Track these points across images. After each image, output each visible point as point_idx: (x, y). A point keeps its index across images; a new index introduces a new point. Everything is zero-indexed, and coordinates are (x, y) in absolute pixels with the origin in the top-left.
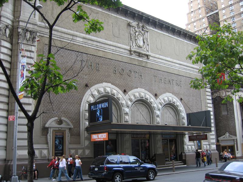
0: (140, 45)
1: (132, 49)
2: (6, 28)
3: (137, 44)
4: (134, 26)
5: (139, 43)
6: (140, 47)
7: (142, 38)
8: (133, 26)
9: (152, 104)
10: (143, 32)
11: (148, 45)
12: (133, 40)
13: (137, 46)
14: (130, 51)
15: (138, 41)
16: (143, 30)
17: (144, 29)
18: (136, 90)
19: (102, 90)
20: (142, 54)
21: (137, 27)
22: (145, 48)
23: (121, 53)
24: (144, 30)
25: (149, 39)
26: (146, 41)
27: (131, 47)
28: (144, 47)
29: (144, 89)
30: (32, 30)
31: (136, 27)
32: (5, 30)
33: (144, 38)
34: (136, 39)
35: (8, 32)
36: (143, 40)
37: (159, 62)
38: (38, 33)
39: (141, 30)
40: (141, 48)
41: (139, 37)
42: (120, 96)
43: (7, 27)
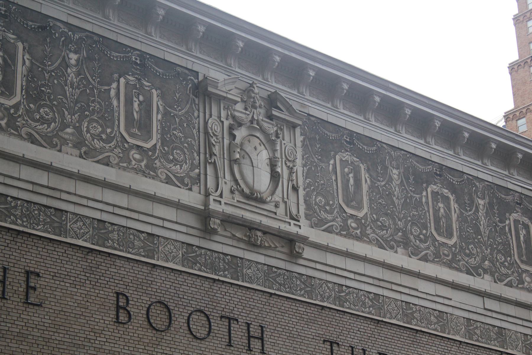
0: (256, 187)
1: (213, 206)
3: (240, 181)
4: (225, 98)
5: (250, 180)
6: (253, 197)
8: (220, 99)
10: (271, 128)
11: (295, 189)
12: (223, 164)
13: (242, 192)
14: (204, 216)
15: (247, 171)
16: (270, 117)
17: (275, 113)
20: (265, 233)
21: (242, 101)
22: (282, 206)
23: (160, 223)
24: (278, 118)
25: (299, 162)
26: (286, 174)
27: (211, 198)
28: (277, 197)
31: (236, 102)
33: (278, 155)
34: (236, 161)
36: (273, 165)
37: (352, 276)
39: (260, 114)
40: (262, 201)
41: (248, 148)
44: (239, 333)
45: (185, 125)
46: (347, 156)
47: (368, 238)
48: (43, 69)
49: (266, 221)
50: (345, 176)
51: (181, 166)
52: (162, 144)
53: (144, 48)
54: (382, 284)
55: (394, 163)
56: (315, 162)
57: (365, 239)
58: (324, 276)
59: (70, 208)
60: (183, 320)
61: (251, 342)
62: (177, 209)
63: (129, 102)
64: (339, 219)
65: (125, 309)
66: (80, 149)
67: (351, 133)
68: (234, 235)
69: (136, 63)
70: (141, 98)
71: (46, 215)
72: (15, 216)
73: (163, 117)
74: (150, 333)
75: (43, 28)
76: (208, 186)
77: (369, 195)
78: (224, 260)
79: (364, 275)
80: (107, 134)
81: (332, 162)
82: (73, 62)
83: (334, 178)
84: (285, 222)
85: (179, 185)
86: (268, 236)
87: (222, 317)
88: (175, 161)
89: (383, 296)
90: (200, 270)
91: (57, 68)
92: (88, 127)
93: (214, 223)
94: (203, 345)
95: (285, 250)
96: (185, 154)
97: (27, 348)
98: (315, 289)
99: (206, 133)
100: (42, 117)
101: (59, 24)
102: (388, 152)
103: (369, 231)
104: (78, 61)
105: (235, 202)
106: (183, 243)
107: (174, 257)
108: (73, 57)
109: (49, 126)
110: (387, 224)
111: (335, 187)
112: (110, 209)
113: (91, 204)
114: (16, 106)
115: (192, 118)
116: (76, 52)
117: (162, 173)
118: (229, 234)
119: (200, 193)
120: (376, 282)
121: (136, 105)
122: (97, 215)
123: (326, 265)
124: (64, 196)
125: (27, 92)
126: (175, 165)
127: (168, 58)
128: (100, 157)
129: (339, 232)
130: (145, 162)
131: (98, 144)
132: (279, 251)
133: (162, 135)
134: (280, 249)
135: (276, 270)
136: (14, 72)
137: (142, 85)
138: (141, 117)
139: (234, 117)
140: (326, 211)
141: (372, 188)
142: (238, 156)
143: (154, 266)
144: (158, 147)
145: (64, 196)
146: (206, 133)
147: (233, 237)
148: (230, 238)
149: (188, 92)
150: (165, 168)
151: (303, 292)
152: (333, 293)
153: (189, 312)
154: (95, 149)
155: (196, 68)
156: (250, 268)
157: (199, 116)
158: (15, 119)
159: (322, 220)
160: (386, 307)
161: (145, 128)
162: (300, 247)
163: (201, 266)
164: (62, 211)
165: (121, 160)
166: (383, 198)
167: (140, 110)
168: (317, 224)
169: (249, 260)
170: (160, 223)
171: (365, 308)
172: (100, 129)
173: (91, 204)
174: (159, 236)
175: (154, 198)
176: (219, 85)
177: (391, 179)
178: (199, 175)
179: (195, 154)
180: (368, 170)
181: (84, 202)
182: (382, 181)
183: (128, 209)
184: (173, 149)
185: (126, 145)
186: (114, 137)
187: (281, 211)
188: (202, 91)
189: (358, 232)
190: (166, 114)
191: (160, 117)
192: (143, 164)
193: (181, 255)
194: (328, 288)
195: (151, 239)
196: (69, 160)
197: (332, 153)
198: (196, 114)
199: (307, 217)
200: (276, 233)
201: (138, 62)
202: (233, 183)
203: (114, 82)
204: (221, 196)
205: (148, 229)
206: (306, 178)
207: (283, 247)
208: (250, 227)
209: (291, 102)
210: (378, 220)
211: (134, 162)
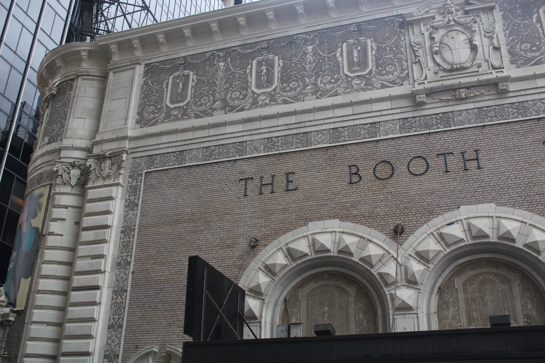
0: (455, 62)
2: (71, 168)
8: (418, 22)
9: (539, 253)
10: (468, 19)
11: (497, 49)
13: (444, 70)
15: (447, 55)
16: (467, 13)
17: (468, 8)
18: (450, 216)
19: (302, 246)
20: (468, 88)
23: (379, 113)
29: (493, 205)
30: (114, 153)
32: (69, 173)
34: (436, 53)
35: (75, 173)
36: (471, 41)
38: (124, 155)
40: (466, 68)
41: (446, 41)
42: (373, 251)
43: (73, 165)
44: (454, 162)
45: (394, 49)
48: (291, 63)
49: (463, 81)
51: (393, 75)
52: (377, 68)
53: (359, 20)
56: (517, 23)
58: (537, 97)
59: (313, 129)
60: (404, 168)
61: (467, 164)
63: (350, 54)
65: (356, 173)
66: (316, 95)
69: (355, 31)
70: (359, 48)
71: (297, 139)
72: (277, 146)
74: (378, 182)
75: (290, 43)
76: (415, 76)
78: (436, 118)
80: (335, 79)
81: (535, 16)
82: (310, 50)
83: (538, 26)
85: (392, 85)
86: (472, 89)
87: (438, 155)
88: (388, 73)
90: (415, 131)
91: (301, 58)
92: (321, 81)
93: (420, 98)
94: (423, 178)
96: (395, 65)
97: (289, 215)
98: (529, 109)
99: (411, 46)
100: (291, 88)
101: (300, 36)
104: (313, 49)
106: (399, 119)
107: (393, 130)
108: (310, 48)
109: (295, 90)
112: (340, 119)
113: (326, 121)
114: (275, 90)
116: (311, 45)
117: (377, 85)
118: (437, 100)
121: (355, 54)
122: (332, 126)
123: (537, 88)
124: (307, 124)
125: (282, 79)
126: (388, 75)
127: (377, 17)
128: (331, 93)
130: (364, 83)
131: (328, 87)
132: (486, 95)
133: (376, 62)
136: (273, 74)
137: (359, 41)
138: (359, 59)
139: (433, 27)
142: (437, 49)
143: (377, 141)
144: (373, 70)
145: (307, 124)
146: (411, 46)
147: (442, 101)
148: (439, 102)
150: (380, 80)
151: (515, 115)
153: (409, 160)
154: (327, 90)
157: (405, 39)
158: (275, 96)
159: (529, 58)
161: (363, 64)
164: (307, 132)
165: (346, 88)
167: (359, 55)
169: (459, 111)
170: (379, 113)
172: (330, 78)
173: (326, 121)
174: (379, 122)
176: (414, 14)
178: (408, 74)
179: (404, 62)
181: (322, 122)
183: (353, 115)
184: (385, 67)
185: (349, 79)
186: (340, 79)
187: (485, 66)
190: (379, 48)
191: (374, 52)
192: (362, 85)
193: (398, 127)
195: (373, 126)
196: (311, 103)
198: (403, 39)
199: (512, 62)
201: (356, 29)
202: (437, 68)
203: (338, 48)
204: (426, 78)
205: (371, 120)
206: (509, 37)
207: (489, 91)
208: (453, 89)
211: (355, 86)
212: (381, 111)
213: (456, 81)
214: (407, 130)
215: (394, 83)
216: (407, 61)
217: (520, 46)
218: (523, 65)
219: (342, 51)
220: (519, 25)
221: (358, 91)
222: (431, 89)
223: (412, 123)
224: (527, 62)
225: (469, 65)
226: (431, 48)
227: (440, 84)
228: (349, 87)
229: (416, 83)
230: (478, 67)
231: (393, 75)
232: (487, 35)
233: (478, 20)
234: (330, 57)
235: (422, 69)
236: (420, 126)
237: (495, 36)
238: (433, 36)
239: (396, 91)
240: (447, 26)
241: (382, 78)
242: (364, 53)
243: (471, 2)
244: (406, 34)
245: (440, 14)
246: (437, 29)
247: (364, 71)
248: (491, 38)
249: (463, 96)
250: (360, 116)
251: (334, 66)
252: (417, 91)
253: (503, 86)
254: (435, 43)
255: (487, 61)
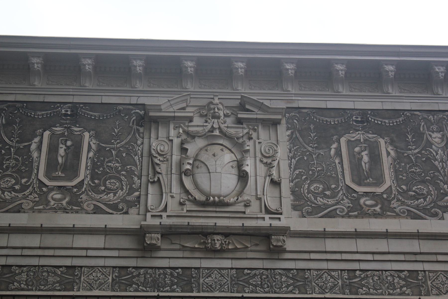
0: (214, 191)
7: (228, 157)
10: (241, 132)
11: (276, 183)
13: (195, 201)
15: (202, 179)
16: (239, 121)
20: (226, 235)
23: (83, 253)
34: (187, 173)
36: (240, 165)
37: (370, 257)
40: (228, 205)
41: (204, 157)
45: (124, 155)
46: (359, 136)
47: (395, 212)
49: (221, 223)
50: (351, 155)
51: (115, 195)
52: (92, 179)
53: (76, 100)
54: (419, 258)
55: (435, 127)
56: (309, 151)
57: (389, 213)
58: (324, 265)
62: (106, 235)
64: (346, 201)
67: (363, 112)
68: (183, 246)
70: (69, 143)
73: (95, 154)
77: (395, 167)
78: (171, 274)
79: (389, 253)
80: (21, 184)
81: (334, 146)
83: (337, 161)
84: (257, 218)
86: (232, 238)
88: (108, 191)
89: (424, 271)
93: (151, 238)
95: (262, 247)
96: (121, 181)
98: (310, 282)
99: (150, 155)
102: (424, 118)
103: (394, 204)
105: (184, 213)
106: (114, 267)
107: (101, 284)
110: (425, 192)
111: (339, 169)
112: (18, 252)
115: (133, 147)
118: (178, 247)
119: (139, 214)
120: (413, 258)
121: (62, 151)
123: (326, 252)
127: (106, 100)
128: (11, 206)
129: (347, 214)
130: (67, 199)
132: (251, 251)
133: (93, 170)
134: (254, 248)
135: (249, 272)
137: (71, 132)
138: (66, 161)
139: (187, 133)
140: (326, 196)
141: (398, 160)
142: (189, 167)
144: (86, 182)
146: (150, 155)
147: (184, 248)
148: (179, 250)
149: (131, 124)
150: (93, 199)
151: (291, 288)
152: (340, 281)
154: (5, 201)
155: (141, 101)
156: (210, 276)
157: (142, 143)
159: (319, 206)
160: (429, 283)
161: (71, 169)
162: (278, 240)
163: (139, 286)
165: (37, 203)
166: (417, 166)
167: (67, 154)
168: (310, 212)
169: (208, 268)
170: (83, 253)
171: (394, 289)
174: (81, 267)
175: (74, 231)
176: (162, 107)
177: (430, 144)
178: (139, 197)
179: (136, 179)
180: (392, 143)
182: (415, 149)
183: (40, 248)
184: (106, 180)
185: (44, 189)
188: (147, 120)
189: (378, 209)
190: (100, 150)
191: (91, 154)
192: (64, 202)
193: (110, 280)
194: (332, 277)
195: (71, 271)
197: (335, 137)
198: (139, 142)
200: (241, 232)
201: (69, 113)
202: (184, 196)
203: (36, 136)
204: (165, 210)
205: (68, 262)
206: (294, 170)
207: (257, 245)
208: (204, 233)
209: (261, 101)
210: (410, 190)
211: (52, 203)
212: (87, 249)
213: (210, 222)
214: (123, 287)
215: (115, 208)
216: (140, 178)
217: (309, 185)
218: (310, 214)
219: (41, 142)
220: (311, 155)
221: (55, 210)
222: (170, 227)
223: (134, 277)
224: (316, 211)
225: (232, 200)
226: (180, 164)
227: (185, 221)
228: (42, 203)
229: (149, 215)
230: (246, 206)
231: (115, 195)
232: (265, 160)
233: (254, 135)
234: (19, 148)
235: (162, 195)
236: (145, 284)
237: (275, 164)
238: (185, 146)
239: (117, 221)
240: (209, 135)
241: (98, 197)
242: (75, 152)
243: (247, 107)
244: (146, 136)
245: (201, 116)
246: (193, 137)
247: (71, 180)
248: (269, 166)
249: (218, 246)
250: (51, 252)
251: (23, 164)
252: (149, 226)
253: (278, 240)
254: (188, 158)
255: (260, 199)
